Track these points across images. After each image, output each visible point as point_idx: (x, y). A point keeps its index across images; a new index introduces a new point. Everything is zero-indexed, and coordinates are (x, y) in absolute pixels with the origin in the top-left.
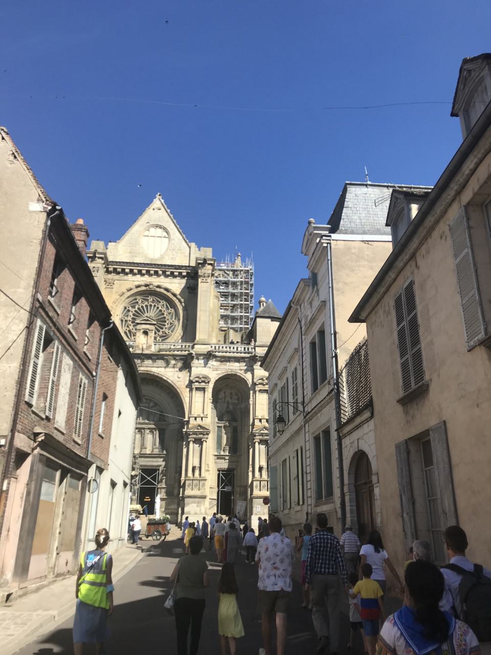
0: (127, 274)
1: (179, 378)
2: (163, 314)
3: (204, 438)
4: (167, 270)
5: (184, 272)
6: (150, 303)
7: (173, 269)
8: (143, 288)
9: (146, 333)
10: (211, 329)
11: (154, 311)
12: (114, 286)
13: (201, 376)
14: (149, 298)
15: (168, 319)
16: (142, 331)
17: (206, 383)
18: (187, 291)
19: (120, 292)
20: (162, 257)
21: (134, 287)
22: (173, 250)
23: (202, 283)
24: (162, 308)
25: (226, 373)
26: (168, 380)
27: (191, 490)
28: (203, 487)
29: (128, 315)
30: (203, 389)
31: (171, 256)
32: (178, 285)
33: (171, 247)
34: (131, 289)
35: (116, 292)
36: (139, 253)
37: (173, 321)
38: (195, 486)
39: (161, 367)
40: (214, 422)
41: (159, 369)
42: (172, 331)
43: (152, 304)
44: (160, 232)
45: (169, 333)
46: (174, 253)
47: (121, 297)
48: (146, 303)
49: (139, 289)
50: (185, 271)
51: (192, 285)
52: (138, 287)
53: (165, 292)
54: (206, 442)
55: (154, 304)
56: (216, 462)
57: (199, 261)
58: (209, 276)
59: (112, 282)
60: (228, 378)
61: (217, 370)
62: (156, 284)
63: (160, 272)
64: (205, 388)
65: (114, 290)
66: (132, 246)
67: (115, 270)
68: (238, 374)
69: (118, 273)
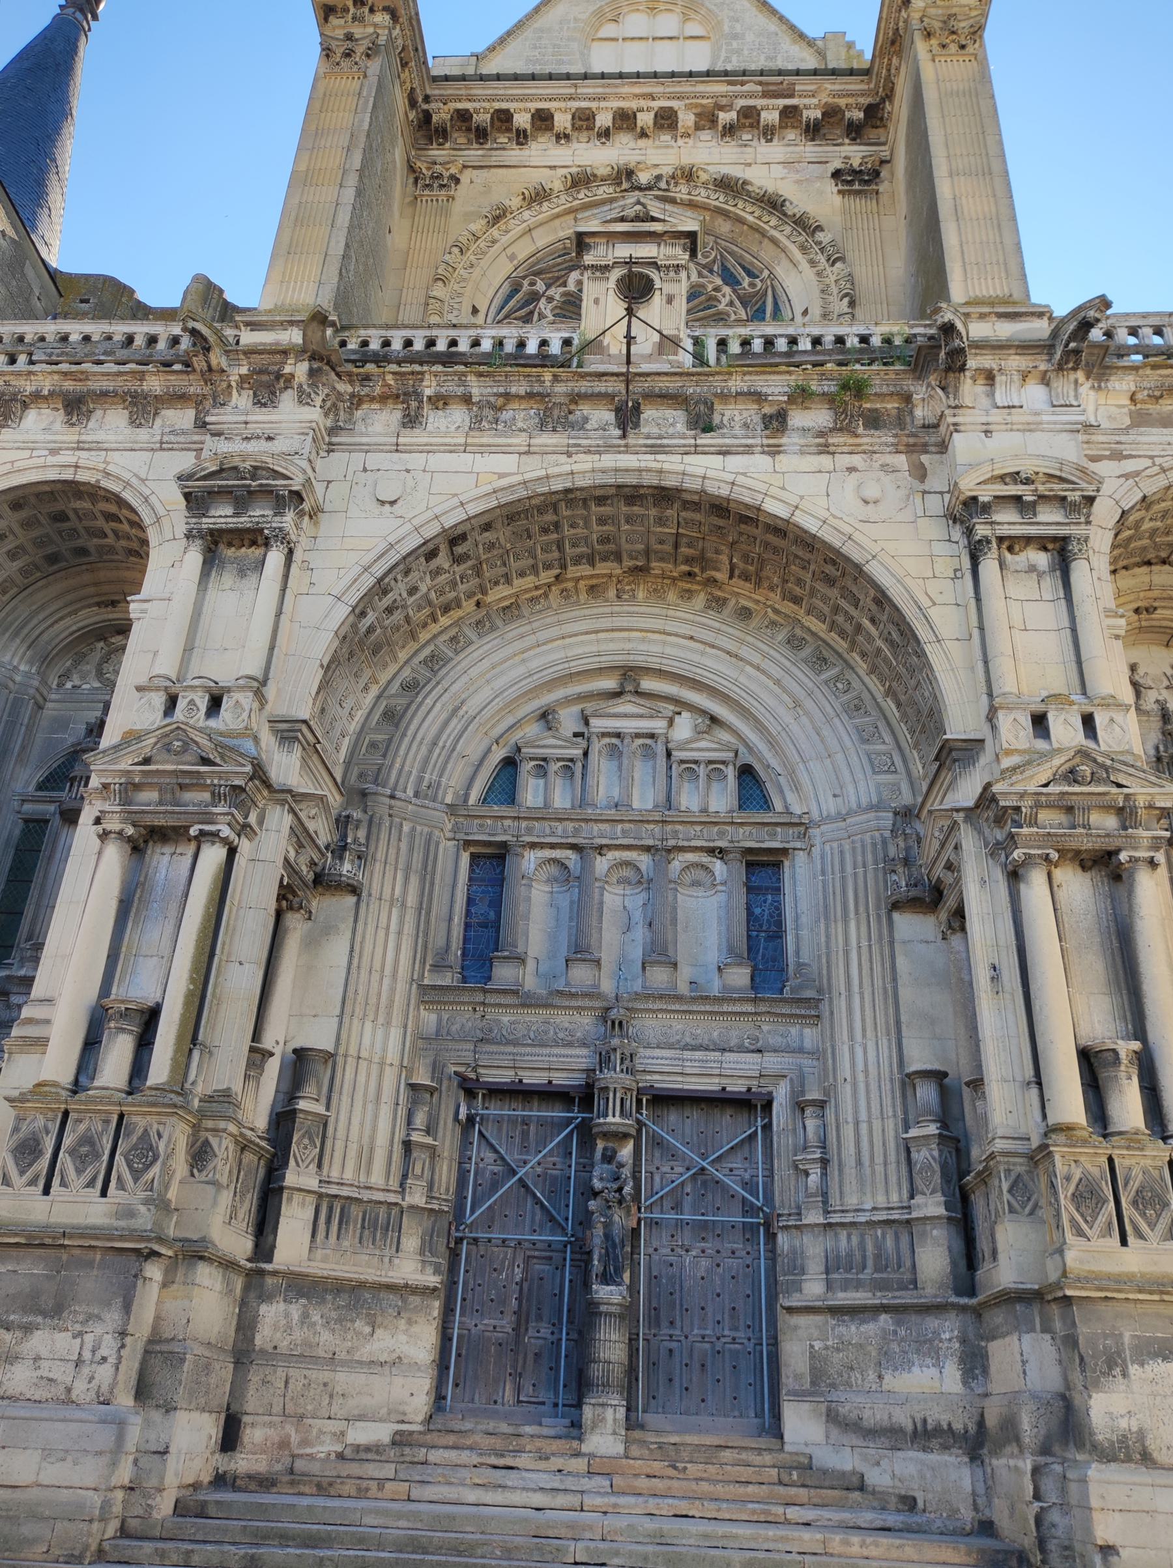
0: (522, 138)
5: (807, 107)
7: (751, 95)
9: (636, 289)
12: (462, 192)
16: (616, 274)
21: (557, 185)
24: (700, 275)
26: (802, 519)
29: (532, 313)
30: (1062, 552)
38: (1135, 1203)
39: (748, 450)
41: (735, 462)
47: (495, 232)
49: (583, 196)
50: (815, 101)
59: (446, 174)
64: (1065, 540)
65: (458, 207)
67: (463, 116)
69: (481, 135)
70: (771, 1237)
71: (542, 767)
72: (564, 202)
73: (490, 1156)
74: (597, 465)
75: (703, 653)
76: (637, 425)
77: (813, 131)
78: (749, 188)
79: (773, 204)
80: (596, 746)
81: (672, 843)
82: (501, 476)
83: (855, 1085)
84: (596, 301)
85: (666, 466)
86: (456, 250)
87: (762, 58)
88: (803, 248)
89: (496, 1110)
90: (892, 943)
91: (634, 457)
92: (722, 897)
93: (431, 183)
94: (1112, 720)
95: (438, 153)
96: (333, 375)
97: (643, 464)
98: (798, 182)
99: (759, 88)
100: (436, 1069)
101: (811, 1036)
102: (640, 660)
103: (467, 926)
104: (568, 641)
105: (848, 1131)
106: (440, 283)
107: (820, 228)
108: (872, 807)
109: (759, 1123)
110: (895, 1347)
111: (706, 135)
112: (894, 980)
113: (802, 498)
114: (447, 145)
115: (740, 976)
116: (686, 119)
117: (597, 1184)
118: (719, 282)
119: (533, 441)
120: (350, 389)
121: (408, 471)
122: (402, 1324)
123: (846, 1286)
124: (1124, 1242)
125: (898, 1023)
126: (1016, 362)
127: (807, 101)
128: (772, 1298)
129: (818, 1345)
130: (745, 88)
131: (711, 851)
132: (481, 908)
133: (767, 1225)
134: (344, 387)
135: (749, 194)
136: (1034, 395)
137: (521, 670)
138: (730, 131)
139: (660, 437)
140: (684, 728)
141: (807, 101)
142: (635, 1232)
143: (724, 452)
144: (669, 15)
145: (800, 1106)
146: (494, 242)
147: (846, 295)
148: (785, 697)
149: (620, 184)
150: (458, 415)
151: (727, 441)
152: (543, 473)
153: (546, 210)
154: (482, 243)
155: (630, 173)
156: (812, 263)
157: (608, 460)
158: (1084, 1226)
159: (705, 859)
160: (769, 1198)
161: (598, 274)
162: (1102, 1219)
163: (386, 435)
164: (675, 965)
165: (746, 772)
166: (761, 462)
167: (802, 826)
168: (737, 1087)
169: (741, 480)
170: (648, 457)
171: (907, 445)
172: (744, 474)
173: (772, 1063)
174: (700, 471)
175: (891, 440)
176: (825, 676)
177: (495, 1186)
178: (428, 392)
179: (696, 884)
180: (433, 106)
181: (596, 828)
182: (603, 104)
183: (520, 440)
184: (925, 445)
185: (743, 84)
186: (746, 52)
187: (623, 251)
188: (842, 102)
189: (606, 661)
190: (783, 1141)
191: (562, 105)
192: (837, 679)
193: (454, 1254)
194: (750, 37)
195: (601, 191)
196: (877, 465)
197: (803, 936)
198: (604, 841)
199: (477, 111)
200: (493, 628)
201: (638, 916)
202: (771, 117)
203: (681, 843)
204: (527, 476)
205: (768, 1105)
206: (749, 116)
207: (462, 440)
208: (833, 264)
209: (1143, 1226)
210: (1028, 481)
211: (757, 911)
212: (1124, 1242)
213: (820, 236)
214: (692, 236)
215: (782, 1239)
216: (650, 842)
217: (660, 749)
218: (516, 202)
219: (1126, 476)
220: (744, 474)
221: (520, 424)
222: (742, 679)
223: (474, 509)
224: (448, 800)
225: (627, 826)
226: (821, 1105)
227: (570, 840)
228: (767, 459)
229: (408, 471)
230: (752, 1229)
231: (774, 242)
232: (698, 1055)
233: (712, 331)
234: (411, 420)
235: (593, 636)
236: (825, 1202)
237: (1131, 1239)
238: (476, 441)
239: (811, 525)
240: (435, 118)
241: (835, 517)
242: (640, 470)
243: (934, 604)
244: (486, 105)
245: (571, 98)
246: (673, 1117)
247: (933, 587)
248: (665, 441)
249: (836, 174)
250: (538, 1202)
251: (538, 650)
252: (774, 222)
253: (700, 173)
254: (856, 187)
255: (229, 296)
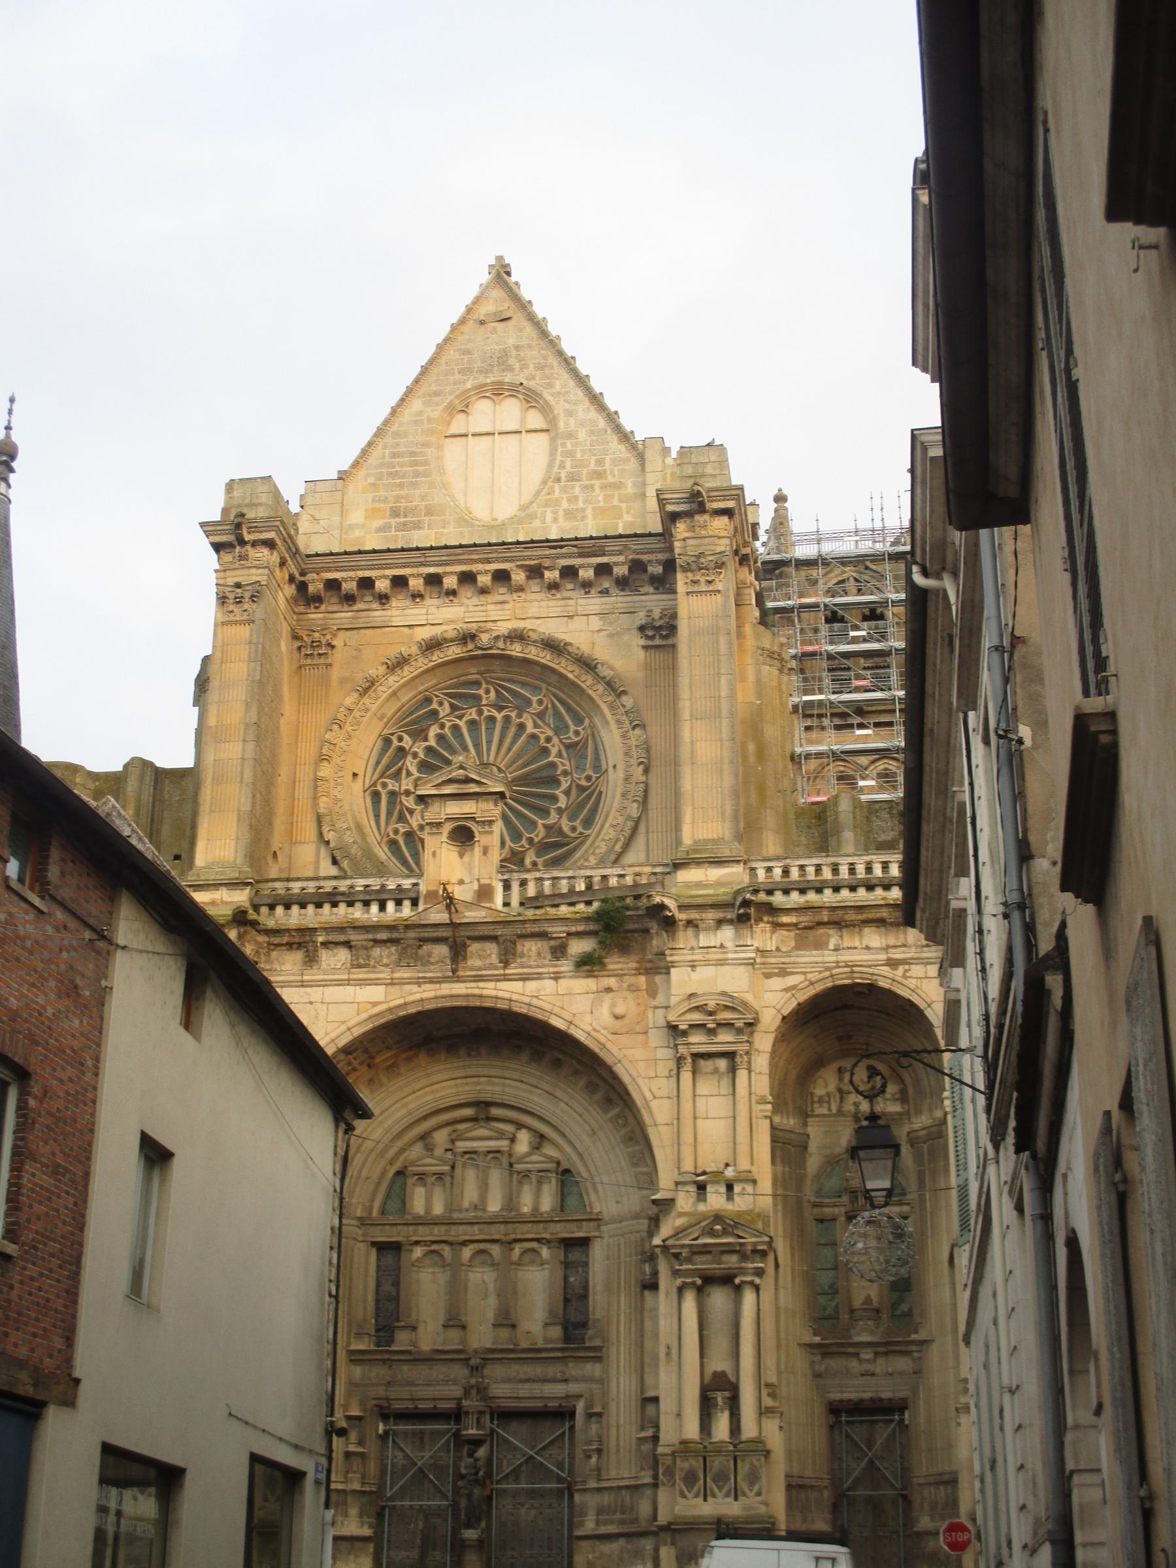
0: (383, 598)
1: (617, 1017)
2: (545, 751)
3: (743, 1271)
4: (547, 563)
5: (616, 564)
6: (486, 713)
8: (454, 652)
9: (463, 835)
10: (754, 798)
11: (508, 741)
12: (338, 656)
13: (712, 1004)
14: (481, 692)
15: (565, 773)
16: (447, 828)
17: (739, 1031)
18: (642, 642)
19: (360, 679)
20: (526, 513)
21: (415, 650)
22: (573, 478)
23: (693, 599)
24: (536, 726)
25: (922, 1005)
26: (574, 1032)
27: (700, 1500)
28: (752, 1483)
29: (399, 771)
31: (565, 504)
32: (595, 623)
33: (562, 466)
34: (402, 662)
35: (343, 681)
36: (429, 511)
37: (588, 778)
38: (714, 1480)
39: (539, 977)
40: (799, 1202)
41: (532, 986)
42: (588, 822)
43: (495, 713)
44: (510, 412)
45: (574, 829)
46: (577, 490)
48: (472, 714)
49: (437, 657)
50: (621, 558)
51: (656, 614)
52: (432, 645)
53: (546, 658)
54: (757, 1288)
55: (503, 713)
56: (817, 1376)
57: (670, 508)
58: (720, 565)
59: (324, 641)
60: (846, 1007)
61: (783, 973)
62: (503, 628)
63: (518, 577)
65: (336, 673)
66: (401, 485)
67: (333, 585)
68: (883, 983)
69: (350, 599)
70: (571, 1496)
71: (422, 1177)
72: (422, 664)
73: (400, 1455)
74: (439, 993)
75: (530, 1092)
76: (465, 958)
77: (623, 583)
78: (569, 648)
79: (587, 665)
80: (460, 1162)
81: (512, 1237)
82: (375, 1004)
83: (618, 1403)
84: (434, 854)
85: (485, 992)
86: (335, 727)
87: (593, 460)
88: (612, 707)
89: (402, 1427)
90: (642, 1311)
91: (462, 985)
92: (546, 1273)
93: (312, 650)
94: (744, 1189)
95: (315, 616)
96: (254, 933)
97: (469, 991)
98: (611, 635)
99: (575, 550)
100: (363, 1403)
101: (595, 1369)
102: (487, 1097)
103: (377, 1301)
104: (436, 1086)
105: (613, 1431)
106: (325, 763)
107: (624, 692)
108: (637, 1216)
109: (567, 1425)
110: (625, 1555)
111: (534, 585)
112: (642, 1336)
113: (574, 1015)
114: (323, 608)
115: (556, 1332)
116: (518, 577)
117: (463, 1471)
118: (550, 733)
119: (397, 975)
120: (266, 939)
121: (311, 1003)
122: (352, 1558)
123: (606, 1523)
124: (705, 1500)
125: (642, 1364)
126: (711, 915)
127: (614, 559)
128: (570, 1530)
129: (590, 1556)
130: (564, 550)
131: (538, 1240)
132: (387, 1287)
133: (569, 1489)
134: (262, 939)
135: (569, 653)
136: (727, 934)
137: (403, 1112)
138: (553, 586)
139: (480, 969)
140: (523, 1143)
141: (614, 559)
142: (490, 1498)
143: (525, 978)
144: (513, 400)
145: (590, 1416)
146: (367, 710)
147: (641, 763)
148: (588, 1128)
149: (465, 643)
150: (343, 955)
151: (526, 970)
152: (401, 1001)
153: (408, 672)
154: (356, 713)
155: (473, 637)
156: (619, 722)
157: (446, 989)
158: (686, 1492)
159: (535, 1245)
160: (571, 1472)
161: (435, 830)
162: (696, 1488)
163: (294, 974)
164: (514, 1326)
165: (565, 1175)
166: (549, 984)
167: (597, 1220)
168: (553, 1404)
169: (535, 1002)
170: (474, 985)
171: (646, 969)
172: (537, 997)
173: (573, 1388)
174: (507, 995)
175: (635, 965)
176: (610, 1115)
177: (404, 1471)
178: (320, 939)
179: (532, 1262)
180: (310, 577)
181: (461, 1228)
182: (448, 569)
183: (385, 975)
184: (657, 968)
185: (561, 547)
186: (578, 455)
187: (455, 808)
188: (645, 558)
189: (463, 1098)
190: (579, 1436)
191: (414, 571)
192: (619, 1116)
193: (380, 1515)
194: (582, 435)
195: (450, 652)
196: (625, 985)
197: (598, 1301)
198: (467, 1238)
199: (345, 580)
200: (381, 1085)
201: (491, 1287)
202: (586, 574)
203: (519, 1236)
204: (393, 1004)
205: (572, 1414)
206: (569, 573)
207: (345, 977)
208: (634, 728)
209: (716, 1490)
210: (711, 1014)
211: (572, 1279)
212: (705, 1500)
213: (624, 699)
214: (502, 795)
215: (577, 1498)
216: (497, 1237)
217: (505, 1160)
218: (382, 669)
219: (787, 990)
220: (537, 997)
221: (385, 961)
222: (558, 1111)
223: (358, 1031)
224: (359, 1214)
225: (481, 1226)
226: (599, 1415)
227: (444, 1238)
228: (552, 982)
229: (311, 1003)
230: (560, 1492)
231: (589, 696)
232: (527, 1386)
233: (516, 876)
234: (311, 960)
235: (452, 1082)
236: (599, 1474)
237: (709, 1498)
238: (355, 976)
239: (581, 1036)
240: (311, 588)
241: (595, 1030)
242: (467, 996)
243: (655, 1097)
244: (351, 574)
245: (422, 564)
246: (514, 1425)
247: (655, 1085)
248: (484, 972)
249: (642, 629)
250: (431, 1481)
251: (414, 1096)
252: (589, 682)
253: (531, 634)
254: (658, 642)
255: (159, 764)
